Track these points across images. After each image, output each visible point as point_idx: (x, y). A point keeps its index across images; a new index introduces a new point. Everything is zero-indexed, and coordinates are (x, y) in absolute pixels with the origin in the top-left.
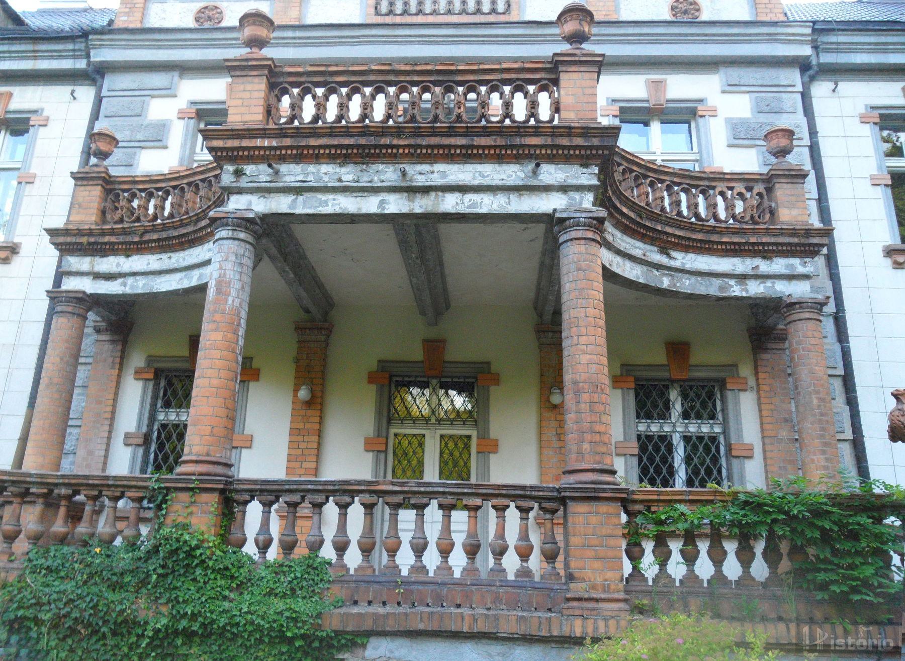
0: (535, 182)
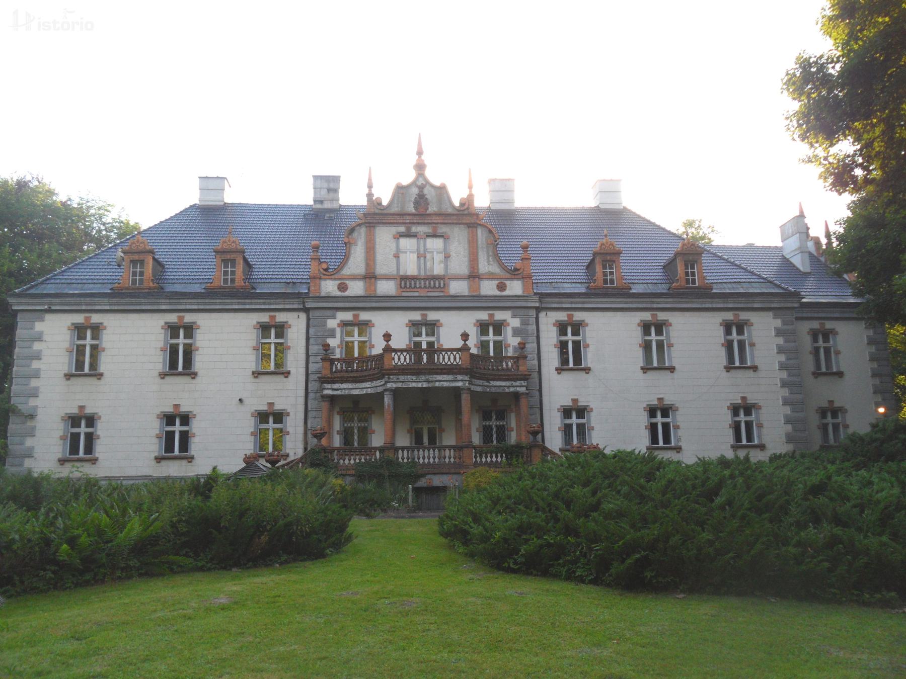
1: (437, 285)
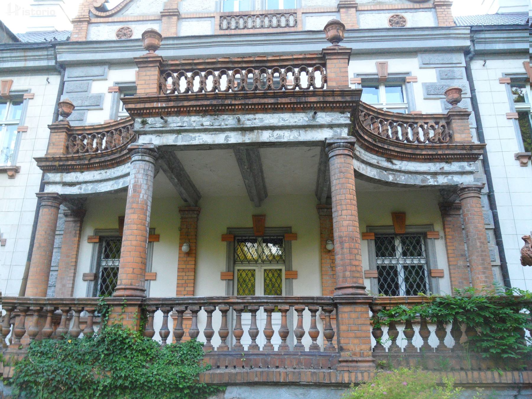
0: (314, 123)
1: (283, 24)
